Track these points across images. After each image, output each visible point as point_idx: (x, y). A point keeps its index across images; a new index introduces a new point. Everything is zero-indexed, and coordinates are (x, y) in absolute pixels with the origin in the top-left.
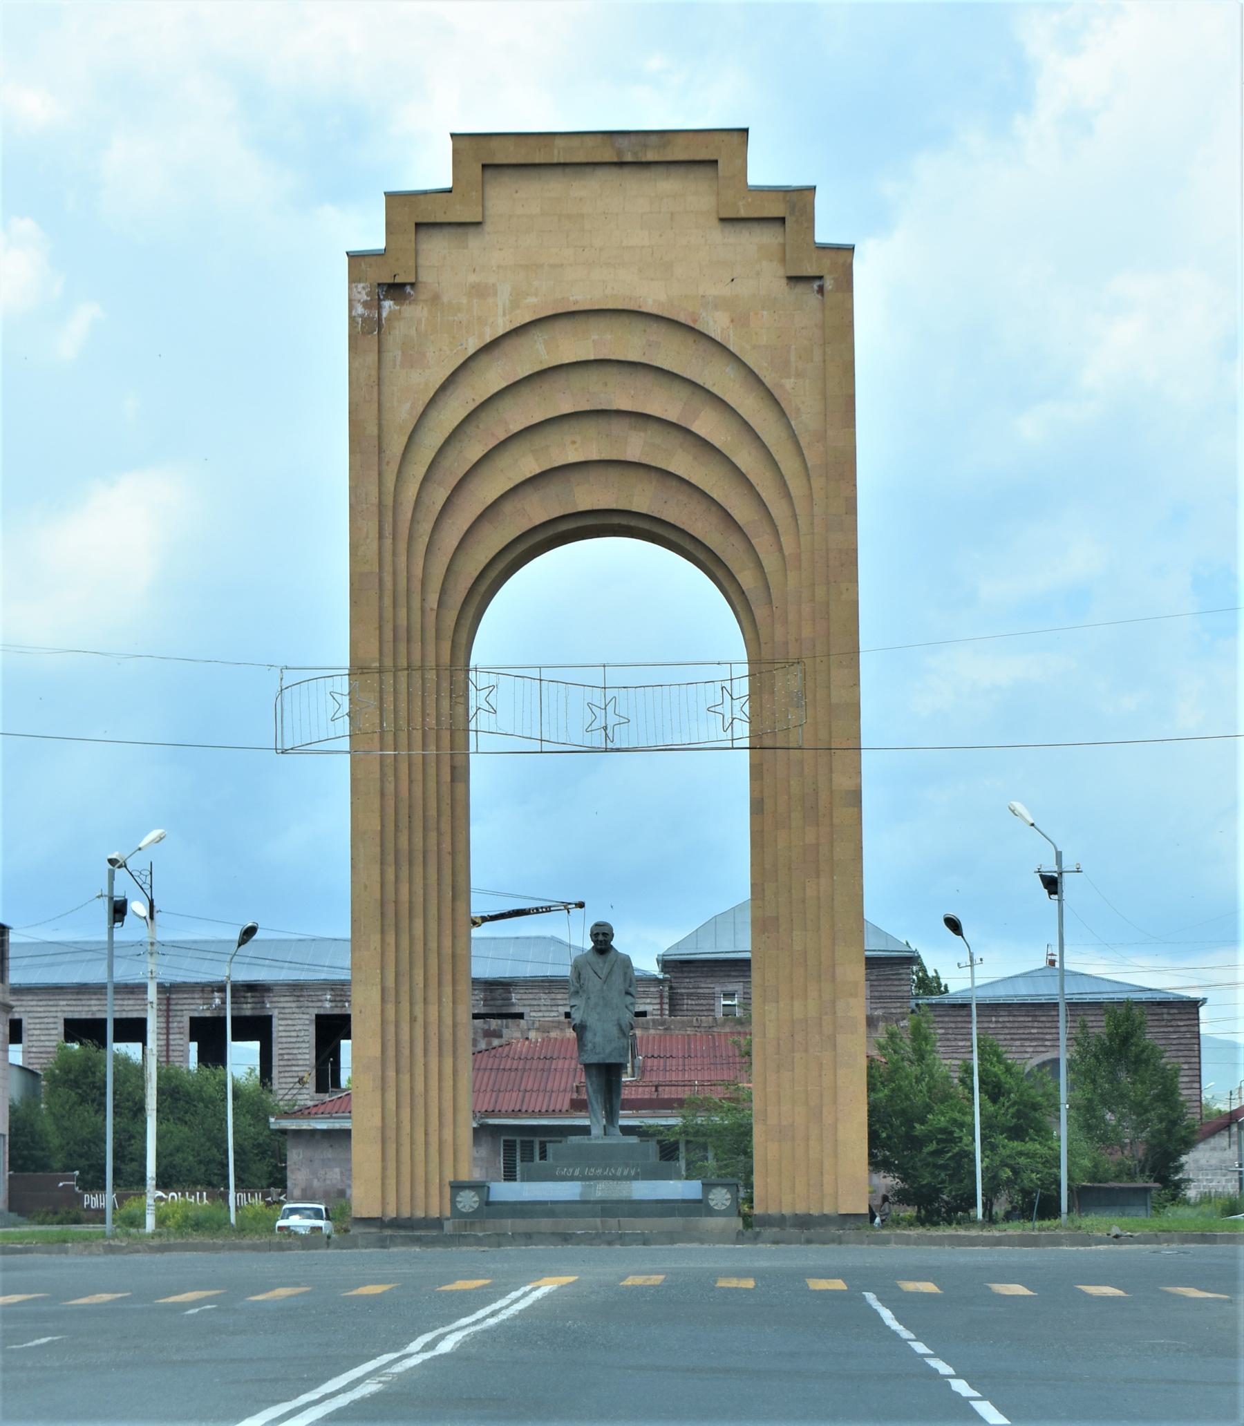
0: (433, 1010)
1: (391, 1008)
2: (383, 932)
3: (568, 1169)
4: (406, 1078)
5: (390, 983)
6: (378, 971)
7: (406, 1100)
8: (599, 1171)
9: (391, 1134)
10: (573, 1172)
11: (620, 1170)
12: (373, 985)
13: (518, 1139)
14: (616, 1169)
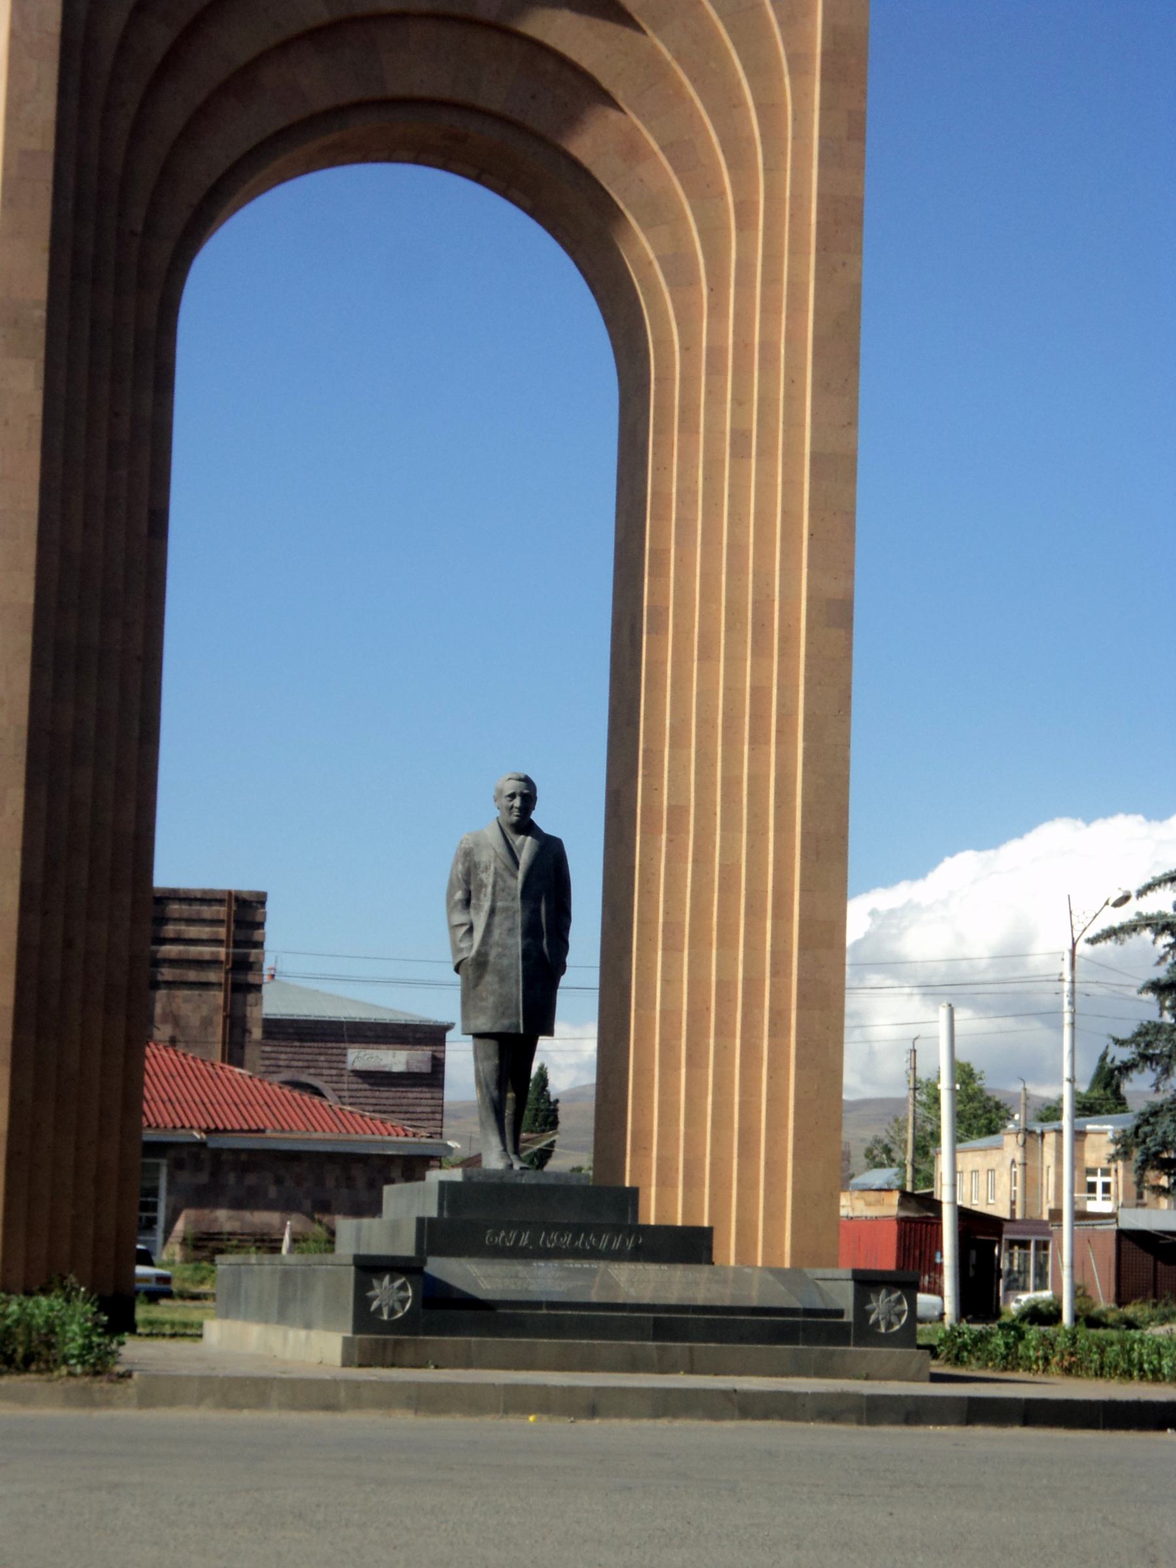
3: (507, 1233)
8: (567, 1239)
11: (605, 1238)
14: (599, 1239)
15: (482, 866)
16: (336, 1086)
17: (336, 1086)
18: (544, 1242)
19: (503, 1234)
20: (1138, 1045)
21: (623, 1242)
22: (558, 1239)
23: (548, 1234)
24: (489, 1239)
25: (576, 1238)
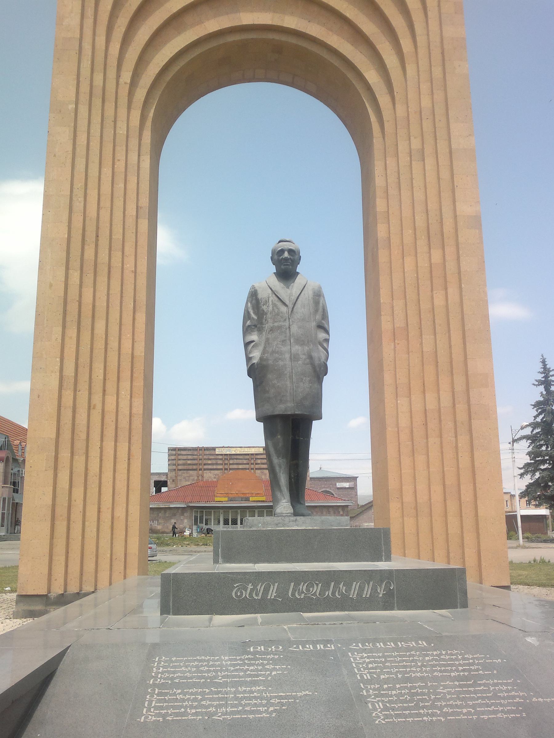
0: (111, 400)
1: (68, 395)
2: (64, 327)
3: (255, 586)
4: (79, 461)
5: (69, 370)
6: (58, 359)
7: (79, 480)
8: (317, 589)
9: (61, 511)
10: (266, 591)
12: (52, 372)
13: (204, 511)
14: (349, 586)
15: (263, 300)
18: (293, 595)
19: (250, 587)
20: (525, 469)
21: (374, 590)
23: (297, 585)
24: (236, 593)
25: (326, 586)
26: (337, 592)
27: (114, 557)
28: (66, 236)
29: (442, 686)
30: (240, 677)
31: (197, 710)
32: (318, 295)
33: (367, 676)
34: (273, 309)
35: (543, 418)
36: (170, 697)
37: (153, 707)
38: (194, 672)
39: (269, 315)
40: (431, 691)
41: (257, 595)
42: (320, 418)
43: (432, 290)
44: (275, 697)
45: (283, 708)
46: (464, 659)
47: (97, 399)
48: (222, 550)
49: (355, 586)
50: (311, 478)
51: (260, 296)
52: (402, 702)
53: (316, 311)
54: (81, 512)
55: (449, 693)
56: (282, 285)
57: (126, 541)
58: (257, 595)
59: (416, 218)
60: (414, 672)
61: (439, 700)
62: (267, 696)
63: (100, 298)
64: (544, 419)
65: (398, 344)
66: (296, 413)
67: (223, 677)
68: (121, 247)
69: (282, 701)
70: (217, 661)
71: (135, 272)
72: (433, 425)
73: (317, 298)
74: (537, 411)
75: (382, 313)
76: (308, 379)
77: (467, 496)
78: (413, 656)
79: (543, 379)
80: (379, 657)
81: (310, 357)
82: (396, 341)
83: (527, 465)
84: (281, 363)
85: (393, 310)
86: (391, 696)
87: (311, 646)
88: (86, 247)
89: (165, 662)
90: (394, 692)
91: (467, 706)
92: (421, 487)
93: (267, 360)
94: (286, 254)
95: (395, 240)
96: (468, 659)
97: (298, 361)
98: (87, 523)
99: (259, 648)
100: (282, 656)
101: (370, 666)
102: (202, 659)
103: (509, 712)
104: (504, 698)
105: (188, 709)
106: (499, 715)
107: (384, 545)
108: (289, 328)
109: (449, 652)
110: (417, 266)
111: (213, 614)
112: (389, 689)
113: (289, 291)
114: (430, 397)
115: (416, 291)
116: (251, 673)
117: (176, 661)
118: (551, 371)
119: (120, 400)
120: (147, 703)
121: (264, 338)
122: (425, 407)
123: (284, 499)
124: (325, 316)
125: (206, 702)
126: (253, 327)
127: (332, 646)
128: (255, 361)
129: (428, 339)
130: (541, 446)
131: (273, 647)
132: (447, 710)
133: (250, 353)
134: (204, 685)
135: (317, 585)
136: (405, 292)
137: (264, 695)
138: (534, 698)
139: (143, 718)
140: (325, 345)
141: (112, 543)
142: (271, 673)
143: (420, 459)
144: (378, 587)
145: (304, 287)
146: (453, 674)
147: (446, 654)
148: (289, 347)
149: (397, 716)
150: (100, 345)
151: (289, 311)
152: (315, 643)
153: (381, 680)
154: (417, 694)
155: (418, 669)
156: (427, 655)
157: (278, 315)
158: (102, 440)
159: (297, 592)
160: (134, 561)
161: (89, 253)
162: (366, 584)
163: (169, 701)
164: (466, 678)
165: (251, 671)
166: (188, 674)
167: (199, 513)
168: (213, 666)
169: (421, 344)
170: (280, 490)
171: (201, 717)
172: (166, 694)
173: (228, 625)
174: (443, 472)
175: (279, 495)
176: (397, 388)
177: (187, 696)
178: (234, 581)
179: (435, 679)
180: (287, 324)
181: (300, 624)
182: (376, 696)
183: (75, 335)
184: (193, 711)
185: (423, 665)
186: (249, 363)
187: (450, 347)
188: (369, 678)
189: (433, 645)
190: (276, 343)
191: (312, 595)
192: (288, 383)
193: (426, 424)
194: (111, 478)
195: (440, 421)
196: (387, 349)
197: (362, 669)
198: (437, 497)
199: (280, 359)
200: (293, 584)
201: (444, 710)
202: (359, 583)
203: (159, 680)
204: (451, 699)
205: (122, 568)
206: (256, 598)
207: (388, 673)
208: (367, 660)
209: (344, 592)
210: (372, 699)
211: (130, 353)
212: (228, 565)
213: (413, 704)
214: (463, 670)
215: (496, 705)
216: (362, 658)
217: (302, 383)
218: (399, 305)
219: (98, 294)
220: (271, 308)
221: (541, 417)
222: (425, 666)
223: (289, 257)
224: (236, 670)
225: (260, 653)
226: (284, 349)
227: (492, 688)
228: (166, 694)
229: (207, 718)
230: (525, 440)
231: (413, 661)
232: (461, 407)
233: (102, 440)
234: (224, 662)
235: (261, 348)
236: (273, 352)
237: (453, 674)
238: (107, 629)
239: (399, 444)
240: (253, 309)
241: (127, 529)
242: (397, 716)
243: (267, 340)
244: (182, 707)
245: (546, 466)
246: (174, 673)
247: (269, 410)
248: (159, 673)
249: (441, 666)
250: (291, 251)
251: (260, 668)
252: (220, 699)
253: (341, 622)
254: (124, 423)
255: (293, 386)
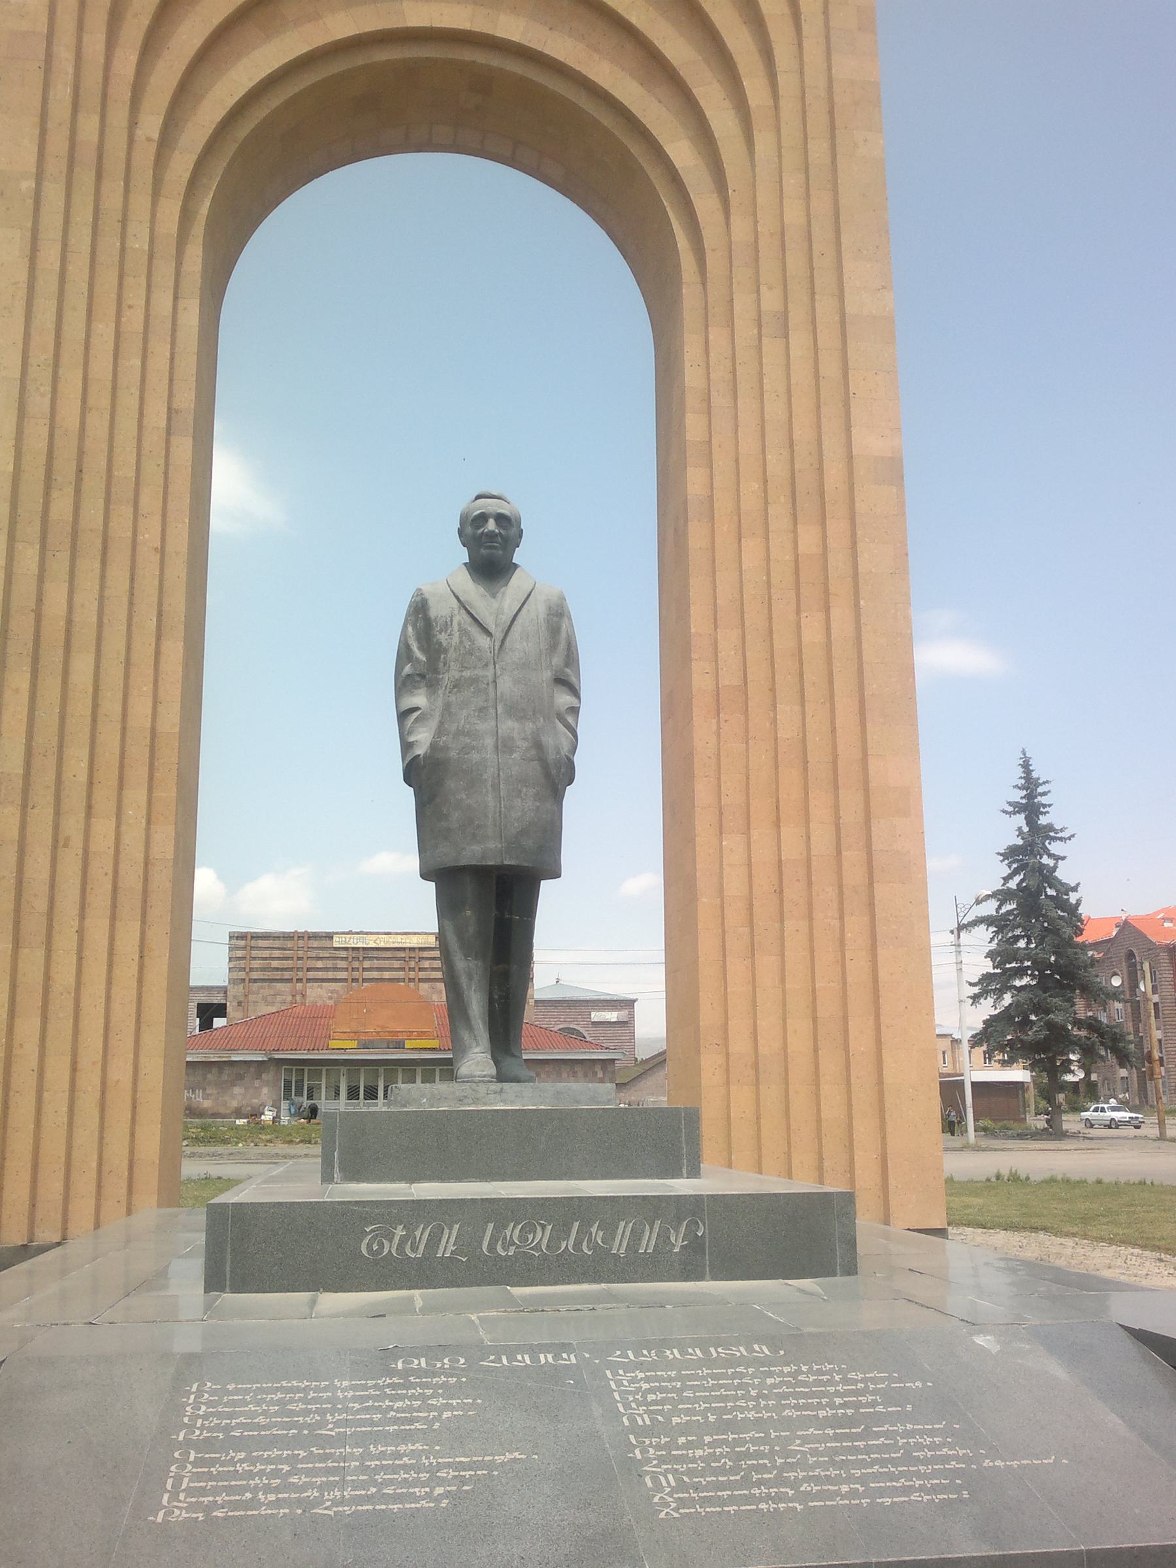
0: (104, 828)
8: (542, 1237)
13: (306, 1069)
14: (610, 1230)
16: (587, 1029)
17: (587, 1029)
18: (492, 1248)
19: (400, 1232)
20: (982, 985)
21: (664, 1237)
22: (523, 1238)
23: (500, 1227)
24: (369, 1246)
25: (562, 1230)
26: (585, 1244)
27: (106, 1168)
28: (11, 468)
29: (799, 1437)
30: (372, 1423)
31: (280, 1496)
32: (557, 615)
33: (643, 1420)
34: (461, 642)
35: (1022, 881)
36: (221, 1469)
37: (184, 1490)
38: (276, 1414)
39: (452, 654)
40: (777, 1448)
41: (414, 1249)
42: (556, 874)
43: (798, 612)
44: (449, 1465)
45: (465, 1488)
46: (845, 1381)
47: (73, 826)
48: (340, 1154)
49: (624, 1229)
50: (536, 1001)
51: (433, 613)
52: (715, 1472)
53: (553, 647)
54: (33, 1070)
55: (814, 1452)
56: (481, 590)
57: (132, 1135)
58: (414, 1249)
59: (769, 457)
60: (742, 1410)
61: (792, 1467)
62: (431, 1464)
63: (82, 606)
64: (1024, 884)
65: (726, 721)
66: (506, 863)
67: (337, 1424)
68: (131, 495)
69: (461, 1473)
70: (325, 1389)
71: (162, 551)
72: (794, 893)
73: (555, 619)
74: (1010, 867)
75: (694, 656)
76: (532, 791)
77: (861, 1042)
78: (741, 1375)
79: (1024, 801)
80: (670, 1379)
81: (538, 746)
82: (721, 715)
83: (987, 978)
84: (475, 756)
85: (716, 648)
86: (694, 1460)
87: (527, 1357)
88: (55, 494)
89: (213, 1392)
90: (699, 1453)
91: (850, 1479)
92: (768, 1022)
93: (446, 748)
94: (491, 525)
95: (723, 504)
96: (855, 1382)
97: (511, 751)
98: (46, 1095)
99: (416, 1362)
100: (464, 1379)
101: (651, 1397)
102: (292, 1387)
103: (935, 1490)
104: (925, 1462)
105: (260, 1493)
106: (915, 1497)
107: (687, 1143)
108: (495, 681)
109: (815, 1367)
110: (768, 558)
111: (318, 1290)
112: (689, 1445)
113: (495, 604)
114: (790, 833)
115: (766, 611)
116: (398, 1415)
117: (236, 1392)
118: (1041, 785)
119: (123, 828)
120: (170, 1481)
121: (440, 703)
122: (780, 855)
123: (478, 1045)
124: (571, 658)
125: (300, 1479)
126: (419, 679)
127: (572, 1357)
128: (420, 751)
129: (787, 711)
130: (1017, 939)
131: (446, 1361)
132: (809, 1489)
133: (410, 733)
134: (297, 1442)
135: (543, 1227)
136: (742, 613)
137: (424, 1461)
138: (987, 1461)
139: (161, 1514)
140: (570, 720)
141: (101, 1138)
142: (440, 1416)
143: (767, 963)
144: (672, 1231)
145: (529, 595)
146: (822, 1413)
147: (810, 1371)
148: (493, 723)
149: (705, 1501)
150: (81, 708)
151: (494, 646)
152: (534, 1351)
153: (673, 1427)
154: (747, 1455)
155: (751, 1404)
156: (770, 1374)
157: (472, 655)
158: (82, 916)
159: (500, 1242)
160: (148, 1178)
161: (62, 506)
162: (647, 1226)
163: (220, 1477)
164: (851, 1422)
165: (398, 1410)
166: (261, 1420)
167: (294, 1075)
168: (315, 1400)
169: (774, 722)
170: (470, 1027)
171: (287, 1511)
172: (213, 1462)
173: (350, 1314)
174: (814, 990)
175: (465, 1035)
176: (721, 814)
177: (259, 1467)
178: (366, 1220)
179: (788, 1423)
180: (489, 673)
181: (505, 1311)
182: (662, 1460)
183: (25, 685)
184: (272, 1497)
185: (760, 1396)
186: (409, 754)
187: (834, 730)
188: (648, 1422)
189: (782, 1353)
190: (464, 713)
191: (531, 1249)
192: (490, 800)
193: (780, 892)
194: (101, 998)
195: (810, 884)
196: (703, 732)
197: (634, 1405)
198: (799, 1044)
199: (473, 748)
200: (491, 1226)
201: (802, 1489)
202: (631, 1224)
203: (198, 1432)
204: (818, 1465)
205: (124, 1191)
206: (413, 1256)
207: (687, 1412)
208: (645, 1386)
209: (599, 1242)
210: (654, 1466)
211: (148, 725)
212: (354, 1186)
213: (738, 1477)
214: (844, 1405)
215: (908, 1475)
216: (633, 1381)
217: (519, 800)
218: (728, 639)
219: (78, 599)
220: (456, 639)
221: (1017, 879)
222: (765, 1397)
223: (497, 531)
224: (366, 1410)
225: (419, 1373)
226: (484, 726)
227: (901, 1442)
228: (213, 1462)
229: (299, 1511)
230: (983, 927)
231: (740, 1386)
232: (853, 856)
233: (82, 916)
234: (339, 1394)
235: (433, 724)
236: (460, 733)
237: (822, 1413)
238: (86, 1324)
239: (724, 932)
240: (419, 640)
241: (134, 1107)
242: (705, 1501)
243: (447, 706)
244: (246, 1489)
245: (1026, 981)
246: (231, 1416)
247: (447, 855)
248: (199, 1416)
249: (796, 1395)
250: (501, 519)
251: (417, 1403)
252: (329, 1471)
253: (591, 1306)
254: (131, 877)
255: (500, 807)
